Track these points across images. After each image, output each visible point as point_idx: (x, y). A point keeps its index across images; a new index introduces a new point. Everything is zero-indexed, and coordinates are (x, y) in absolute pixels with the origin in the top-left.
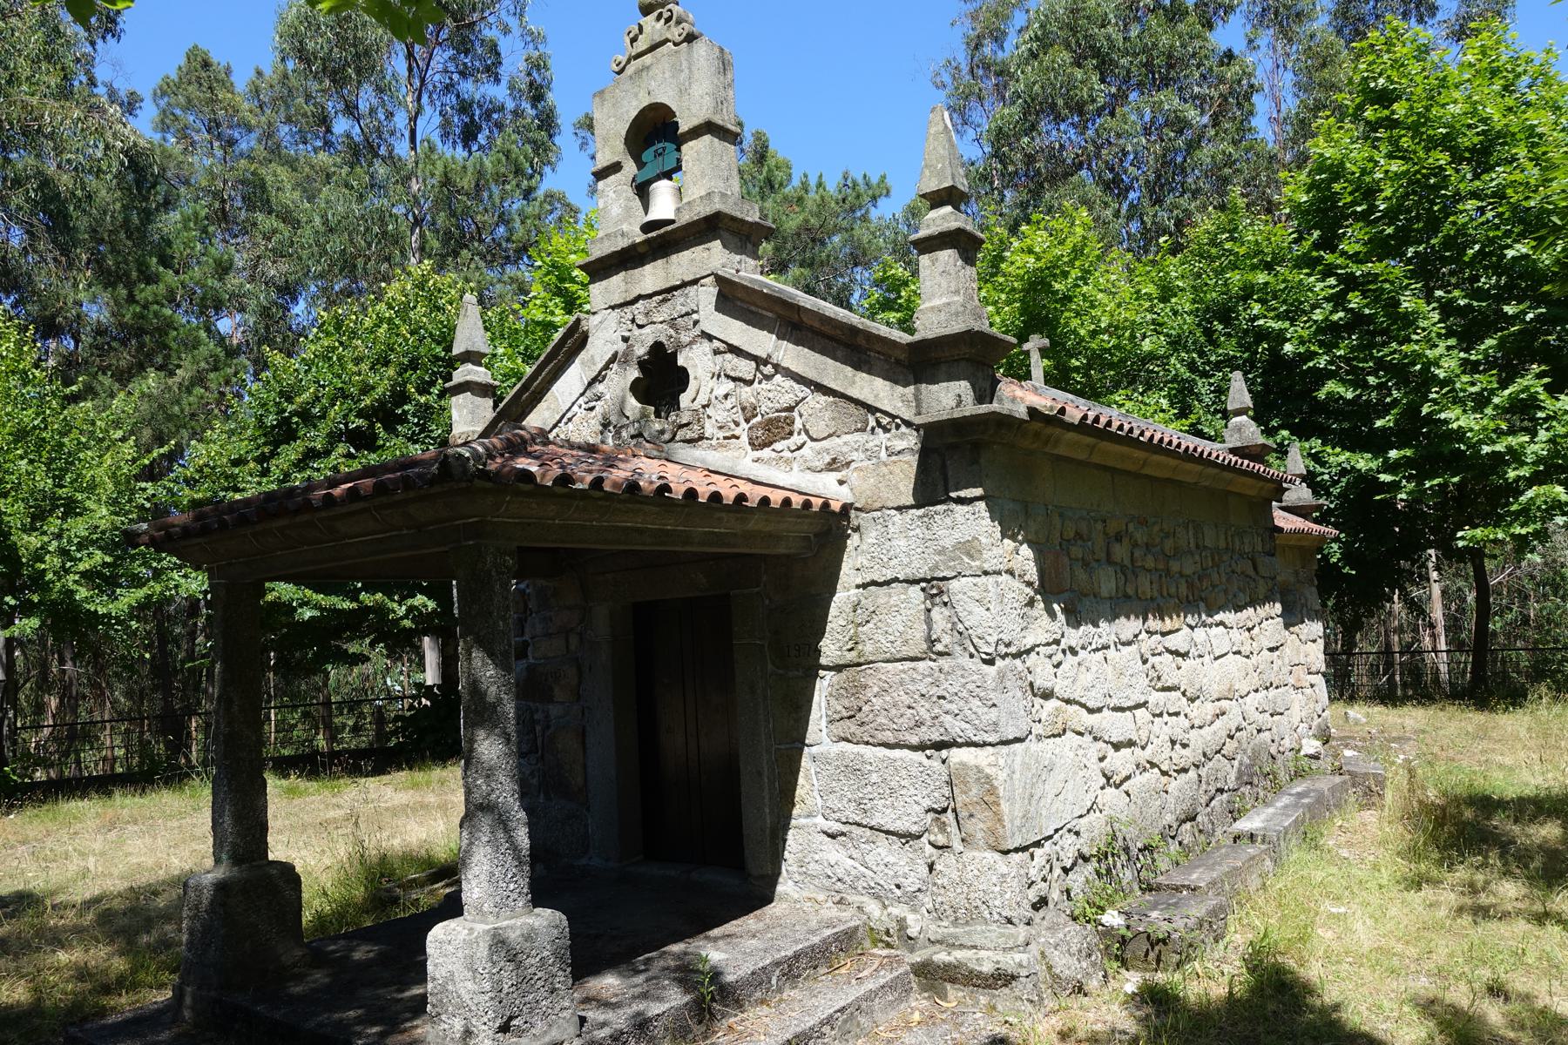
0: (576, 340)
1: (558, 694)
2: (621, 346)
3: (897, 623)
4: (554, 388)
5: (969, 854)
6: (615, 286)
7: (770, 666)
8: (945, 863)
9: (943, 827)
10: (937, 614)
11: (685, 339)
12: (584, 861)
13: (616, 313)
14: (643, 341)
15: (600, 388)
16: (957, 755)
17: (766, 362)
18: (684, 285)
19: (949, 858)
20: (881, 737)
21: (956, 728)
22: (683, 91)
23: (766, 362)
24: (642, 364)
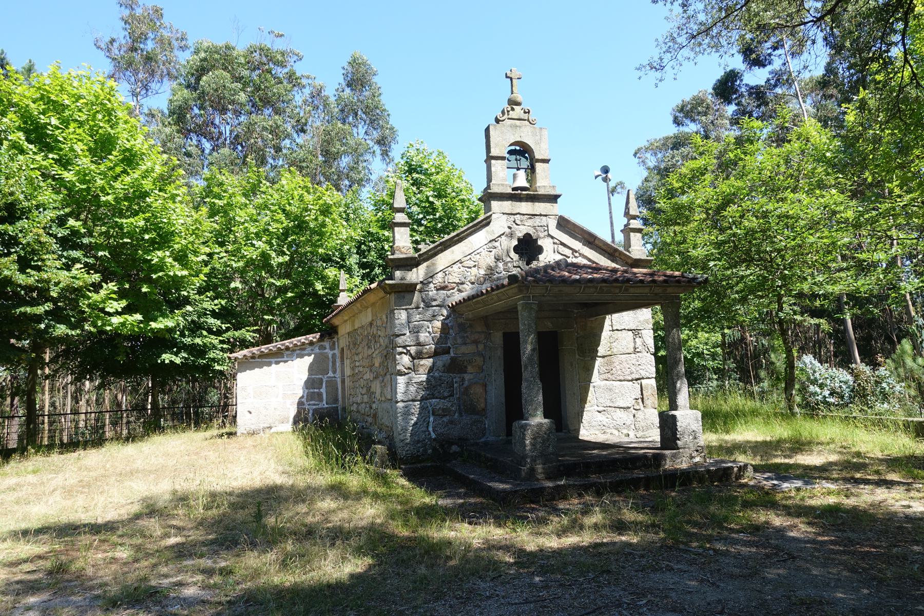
0: (487, 222)
1: (470, 369)
2: (508, 231)
3: (624, 343)
4: (470, 238)
5: (646, 410)
6: (507, 206)
7: (577, 356)
8: (639, 415)
9: (638, 404)
10: (637, 340)
11: (542, 235)
12: (483, 440)
13: (505, 216)
14: (521, 232)
15: (497, 244)
16: (644, 382)
17: (576, 252)
18: (541, 215)
19: (639, 412)
20: (618, 378)
21: (644, 374)
22: (537, 143)
23: (576, 252)
24: (519, 240)
